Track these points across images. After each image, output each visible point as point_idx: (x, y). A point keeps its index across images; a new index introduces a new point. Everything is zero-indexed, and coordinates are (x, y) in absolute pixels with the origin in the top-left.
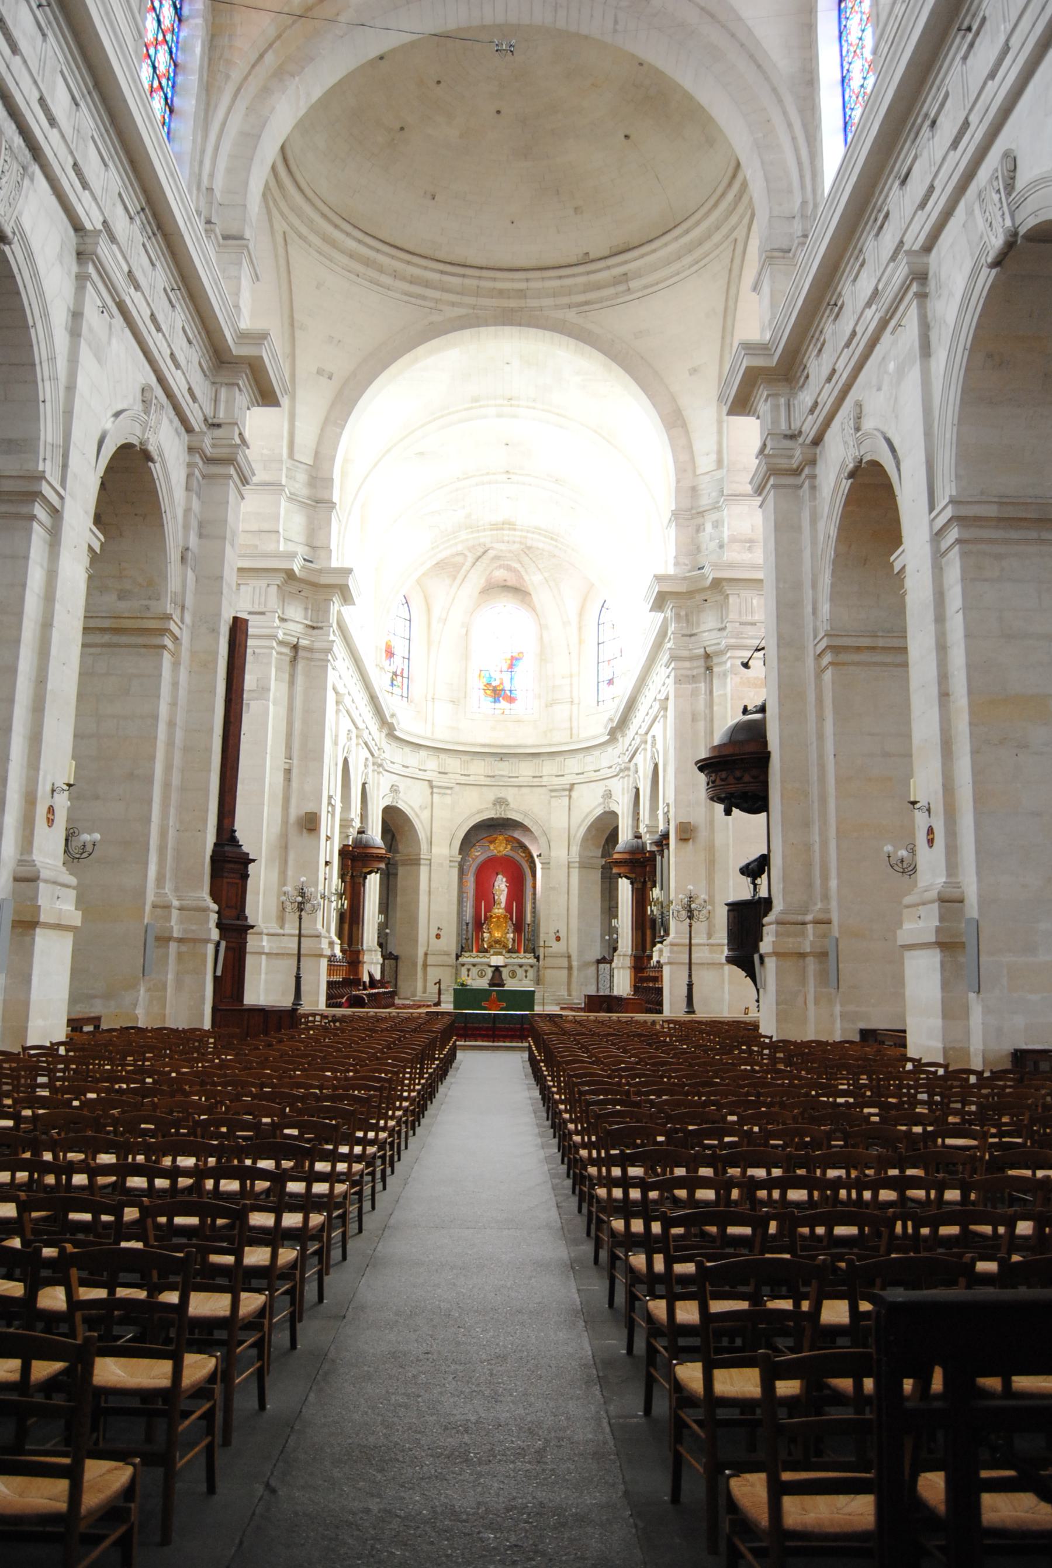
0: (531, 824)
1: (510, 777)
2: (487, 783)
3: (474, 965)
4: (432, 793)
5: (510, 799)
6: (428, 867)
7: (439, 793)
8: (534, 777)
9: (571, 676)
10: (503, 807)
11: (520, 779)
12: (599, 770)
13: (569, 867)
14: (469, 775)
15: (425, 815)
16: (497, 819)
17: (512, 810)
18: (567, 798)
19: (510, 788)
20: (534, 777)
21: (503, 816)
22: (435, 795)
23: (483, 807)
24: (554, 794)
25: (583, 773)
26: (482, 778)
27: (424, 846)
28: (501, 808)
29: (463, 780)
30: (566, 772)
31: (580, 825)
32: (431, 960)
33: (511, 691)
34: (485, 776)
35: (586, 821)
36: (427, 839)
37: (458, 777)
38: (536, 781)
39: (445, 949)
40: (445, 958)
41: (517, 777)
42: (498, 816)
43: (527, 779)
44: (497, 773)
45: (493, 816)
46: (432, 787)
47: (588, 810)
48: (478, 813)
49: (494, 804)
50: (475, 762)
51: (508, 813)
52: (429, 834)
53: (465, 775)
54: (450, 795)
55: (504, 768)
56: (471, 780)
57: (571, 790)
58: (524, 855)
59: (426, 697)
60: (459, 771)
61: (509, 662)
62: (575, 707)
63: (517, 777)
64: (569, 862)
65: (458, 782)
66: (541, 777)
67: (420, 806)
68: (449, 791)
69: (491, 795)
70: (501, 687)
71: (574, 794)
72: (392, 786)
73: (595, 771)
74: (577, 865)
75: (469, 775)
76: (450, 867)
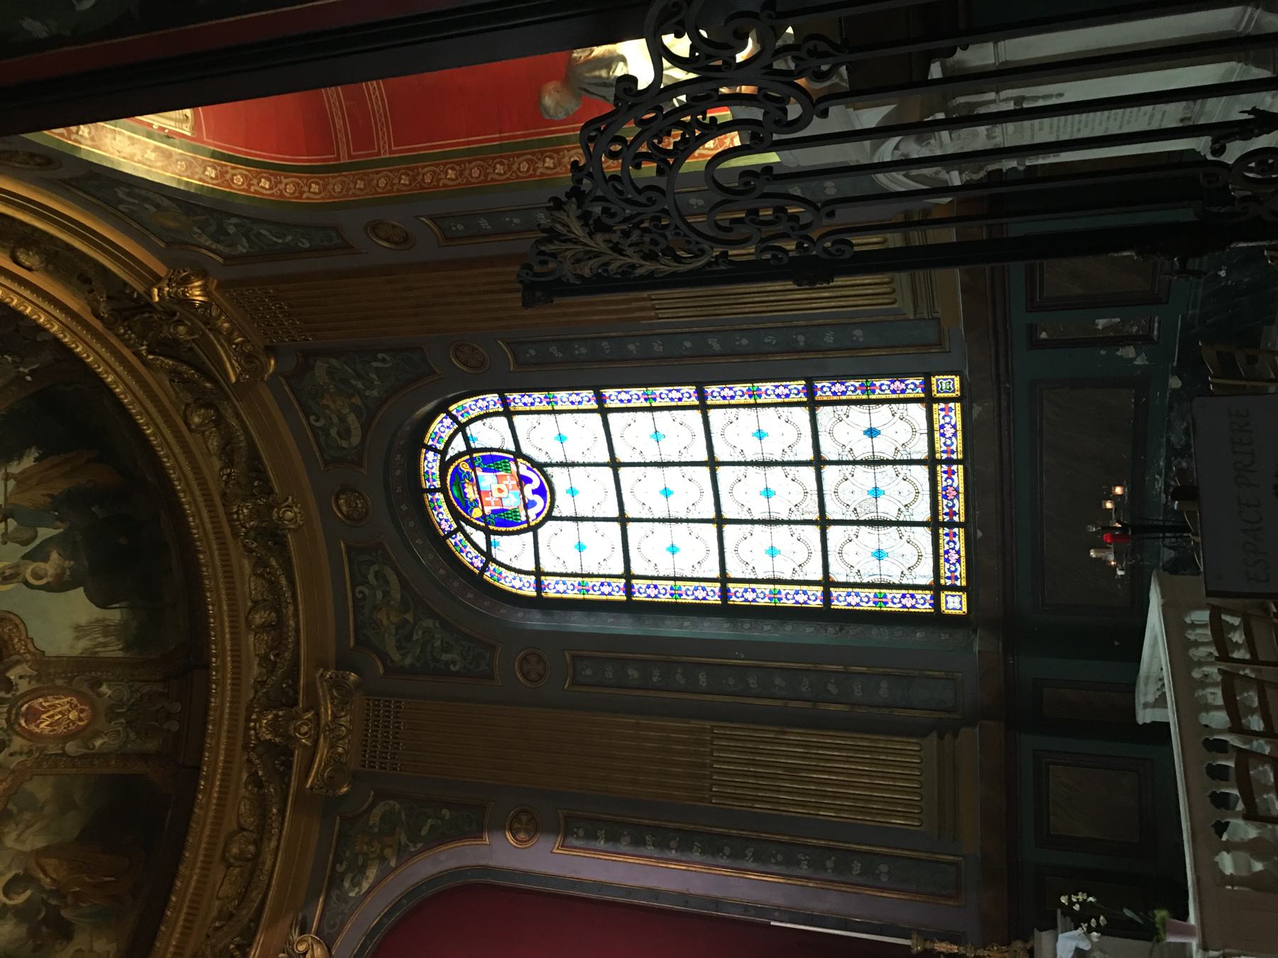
58: (372, 873)
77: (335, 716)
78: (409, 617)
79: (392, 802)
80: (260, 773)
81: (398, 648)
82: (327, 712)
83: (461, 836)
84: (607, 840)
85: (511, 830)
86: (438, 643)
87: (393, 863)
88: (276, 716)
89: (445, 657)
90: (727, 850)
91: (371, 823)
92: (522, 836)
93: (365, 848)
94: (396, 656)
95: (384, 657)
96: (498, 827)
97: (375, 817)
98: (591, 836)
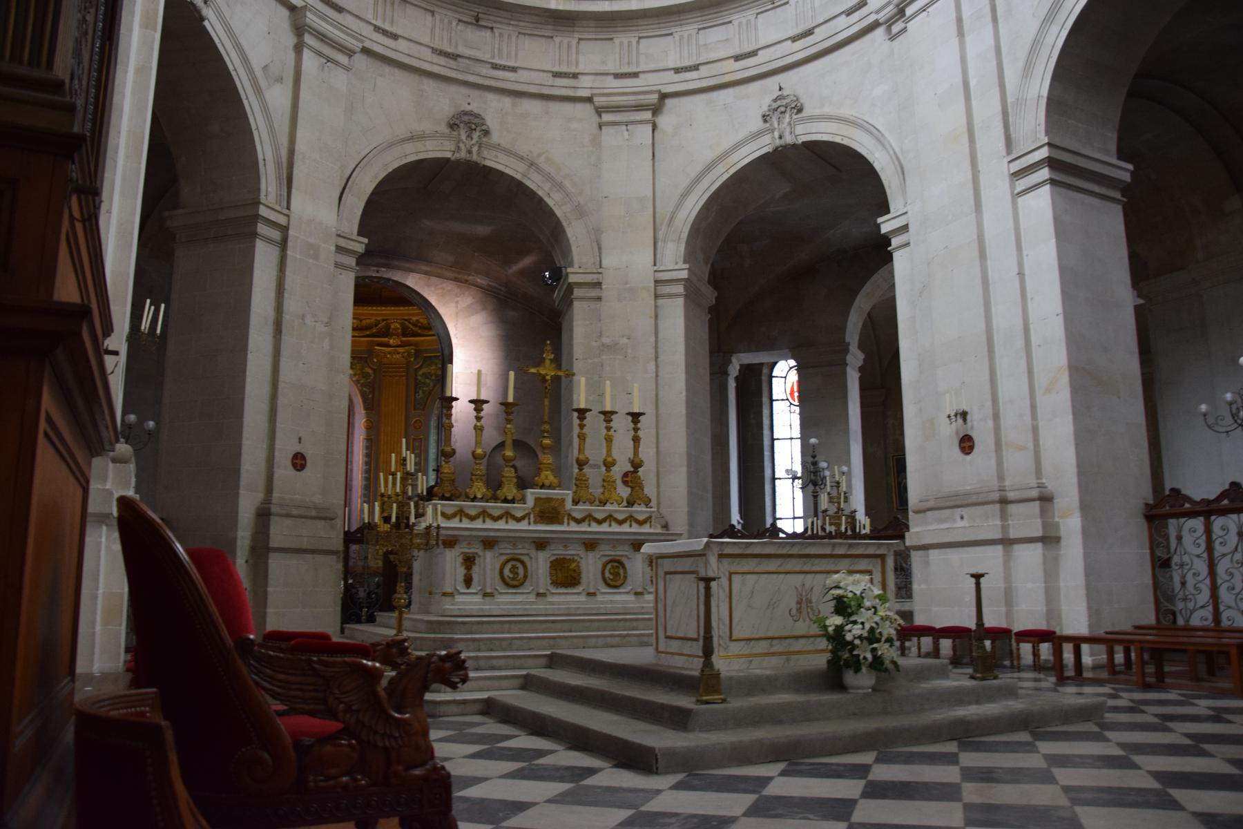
1: (495, 67)
2: (436, 69)
3: (489, 543)
4: (299, 48)
5: (491, 122)
6: (274, 252)
7: (319, 53)
8: (557, 75)
10: (476, 136)
11: (521, 76)
12: (753, 54)
13: (656, 297)
14: (395, 37)
15: (278, 97)
16: (458, 164)
17: (498, 147)
18: (650, 127)
19: (491, 96)
20: (557, 75)
21: (475, 157)
22: (307, 55)
23: (427, 127)
24: (607, 117)
25: (695, 68)
26: (427, 54)
28: (469, 137)
29: (379, 44)
30: (643, 67)
32: (280, 533)
34: (434, 50)
35: (705, 183)
36: (278, 164)
37: (367, 31)
38: (562, 87)
39: (318, 499)
40: (319, 528)
41: (514, 69)
42: (463, 155)
44: (461, 50)
45: (448, 155)
46: (299, 29)
47: (710, 155)
48: (412, 138)
49: (453, 126)
51: (485, 153)
52: (284, 153)
53: (385, 33)
54: (347, 69)
56: (401, 50)
57: (656, 109)
60: (370, 17)
63: (514, 69)
64: (656, 282)
65: (368, 44)
66: (575, 76)
67: (265, 68)
68: (342, 59)
69: (446, 101)
71: (664, 121)
73: (738, 58)
74: (680, 289)
75: (395, 37)
76: (338, 265)
77: (399, 353)
78: (433, 378)
79: (373, 375)
80: (380, 325)
81: (423, 374)
82: (401, 350)
83: (364, 402)
84: (367, 453)
85: (367, 420)
86: (425, 389)
87: (354, 379)
88: (398, 329)
89: (421, 392)
90: (366, 492)
91: (366, 369)
92: (365, 424)
93: (358, 368)
94: (421, 373)
95: (421, 368)
96: (368, 416)
97: (368, 370)
98: (367, 448)
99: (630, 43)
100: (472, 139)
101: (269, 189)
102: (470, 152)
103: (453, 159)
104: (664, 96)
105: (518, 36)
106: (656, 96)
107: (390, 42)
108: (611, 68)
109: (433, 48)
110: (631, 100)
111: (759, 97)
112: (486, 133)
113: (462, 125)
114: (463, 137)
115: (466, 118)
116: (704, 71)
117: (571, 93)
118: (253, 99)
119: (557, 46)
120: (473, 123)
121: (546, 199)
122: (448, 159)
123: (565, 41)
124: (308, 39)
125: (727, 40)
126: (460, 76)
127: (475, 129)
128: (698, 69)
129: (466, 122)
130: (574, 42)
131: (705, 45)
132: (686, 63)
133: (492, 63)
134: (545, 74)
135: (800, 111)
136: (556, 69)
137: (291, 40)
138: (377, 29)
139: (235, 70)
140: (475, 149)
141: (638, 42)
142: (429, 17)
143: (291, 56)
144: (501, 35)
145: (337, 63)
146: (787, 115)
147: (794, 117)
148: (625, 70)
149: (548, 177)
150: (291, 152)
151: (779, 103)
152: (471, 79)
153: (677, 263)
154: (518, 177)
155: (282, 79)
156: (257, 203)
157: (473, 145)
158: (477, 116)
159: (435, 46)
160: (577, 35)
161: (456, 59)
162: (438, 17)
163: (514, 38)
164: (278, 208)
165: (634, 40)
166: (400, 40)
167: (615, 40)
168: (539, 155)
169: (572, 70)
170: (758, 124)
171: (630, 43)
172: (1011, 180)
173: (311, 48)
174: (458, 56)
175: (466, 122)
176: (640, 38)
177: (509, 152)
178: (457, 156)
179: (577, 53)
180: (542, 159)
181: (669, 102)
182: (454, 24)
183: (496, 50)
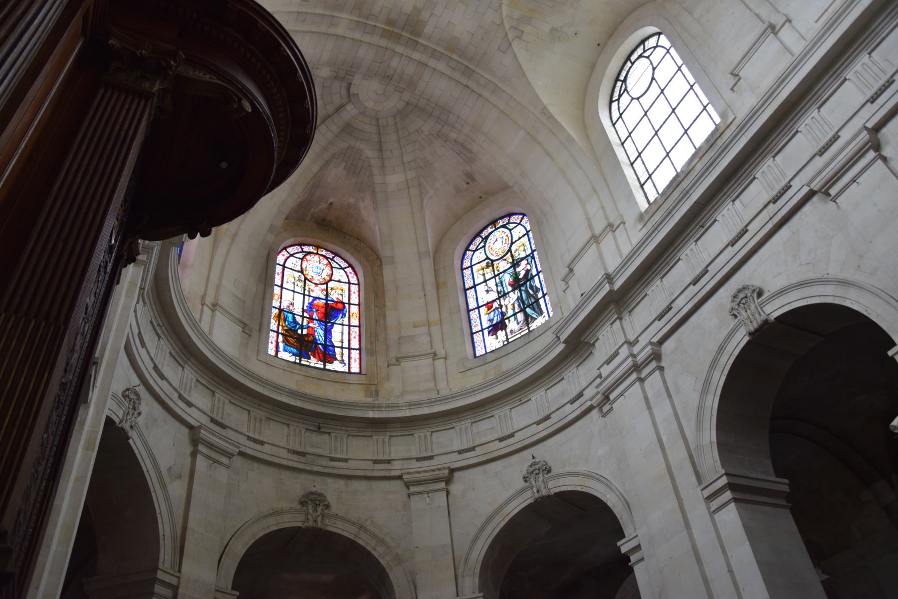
0: (373, 543)
1: (333, 459)
2: (291, 464)
4: (194, 455)
5: (331, 498)
8: (376, 462)
9: (429, 324)
10: (320, 509)
11: (351, 464)
12: (511, 435)
14: (262, 443)
15: (177, 490)
17: (336, 516)
18: (444, 494)
19: (330, 480)
20: (376, 462)
21: (320, 525)
22: (200, 459)
24: (413, 489)
25: (473, 449)
26: (284, 453)
27: (166, 555)
28: (315, 510)
29: (251, 448)
30: (436, 452)
31: (475, 540)
33: (325, 346)
34: (289, 451)
35: (489, 529)
36: (174, 539)
37: (243, 440)
38: (380, 470)
41: (346, 460)
42: (310, 523)
43: (362, 464)
44: (309, 449)
45: (300, 524)
46: (195, 441)
47: (490, 510)
49: (303, 503)
50: (273, 425)
51: (327, 521)
53: (255, 441)
54: (228, 467)
55: (321, 444)
57: (448, 480)
59: (203, 298)
60: (244, 431)
61: (323, 310)
62: (439, 363)
63: (346, 460)
65: (243, 449)
66: (389, 462)
67: (170, 469)
68: (225, 460)
69: (297, 486)
70: (311, 338)
71: (455, 488)
72: (128, 390)
73: (501, 440)
75: (262, 443)
99: (425, 436)
100: (317, 512)
101: (166, 557)
102: (315, 521)
103: (303, 527)
104: (452, 471)
105: (347, 438)
106: (447, 471)
107: (259, 447)
108: (414, 454)
109: (288, 449)
110: (430, 475)
111: (519, 466)
112: (327, 506)
113: (309, 502)
114: (311, 511)
115: (312, 497)
116: (479, 451)
117: (387, 474)
118: (159, 492)
119: (375, 442)
120: (317, 500)
121: (373, 552)
122: (300, 527)
123: (381, 438)
124: (201, 448)
125: (493, 428)
126: (308, 468)
127: (319, 505)
128: (474, 450)
129: (313, 500)
130: (387, 439)
131: (477, 433)
132: (466, 446)
133: (330, 457)
134: (368, 462)
135: (549, 471)
136: (375, 458)
137: (189, 449)
138: (249, 438)
139: (148, 471)
140: (319, 519)
141: (431, 435)
142: (286, 429)
143: (189, 460)
144: (336, 438)
145: (220, 463)
146: (541, 476)
147: (546, 476)
148: (424, 455)
149: (374, 536)
150: (184, 529)
151: (534, 467)
152: (316, 469)
153: (474, 593)
154: (352, 537)
155: (181, 476)
156: (156, 568)
157: (318, 516)
158: (320, 495)
159: (290, 448)
160: (388, 434)
161: (305, 456)
162: (292, 428)
163: (345, 439)
164: (172, 572)
165: (428, 434)
166: (266, 445)
167: (415, 435)
168: (366, 520)
169: (387, 457)
170: (521, 484)
171: (425, 436)
172: (706, 503)
173: (202, 454)
174: (306, 453)
175: (313, 500)
176: (432, 432)
177: (344, 520)
178: (307, 524)
179: (389, 446)
180: (369, 522)
181: (457, 475)
182: (303, 432)
183: (333, 448)
